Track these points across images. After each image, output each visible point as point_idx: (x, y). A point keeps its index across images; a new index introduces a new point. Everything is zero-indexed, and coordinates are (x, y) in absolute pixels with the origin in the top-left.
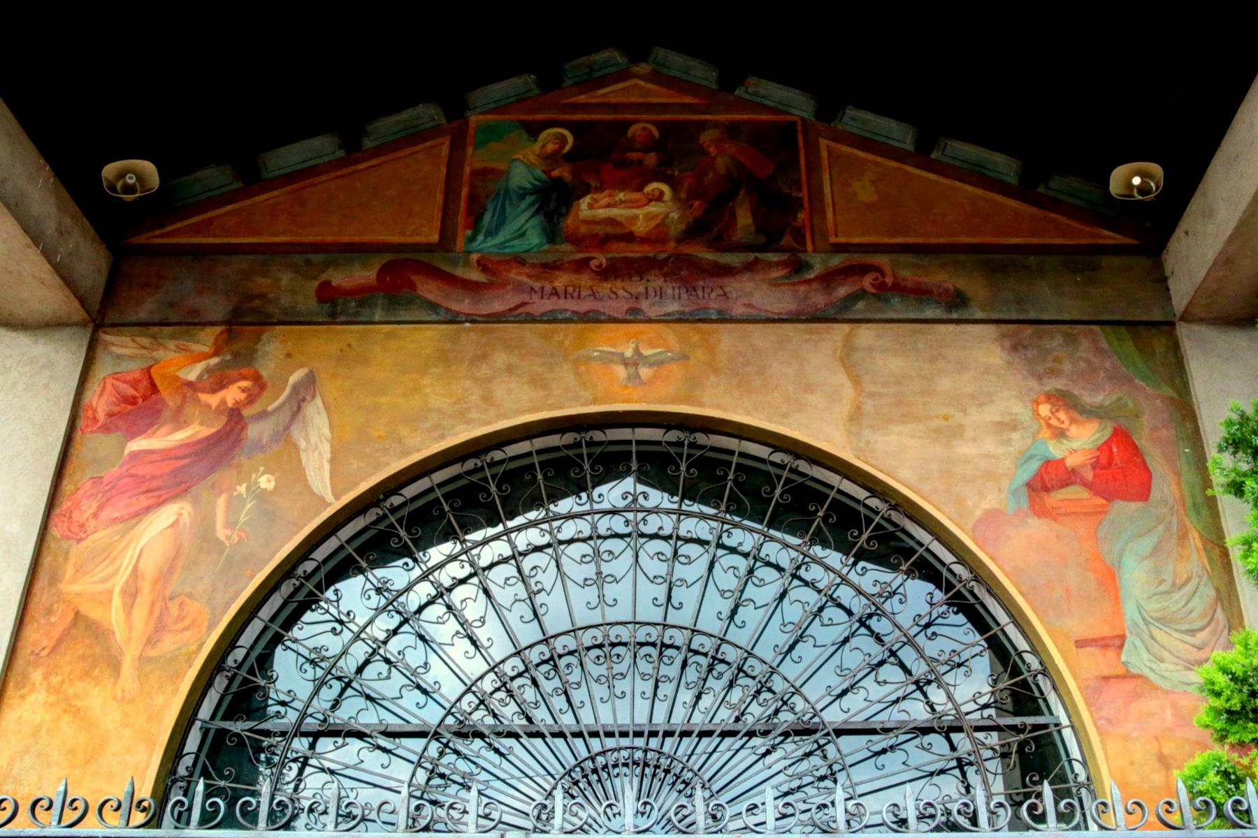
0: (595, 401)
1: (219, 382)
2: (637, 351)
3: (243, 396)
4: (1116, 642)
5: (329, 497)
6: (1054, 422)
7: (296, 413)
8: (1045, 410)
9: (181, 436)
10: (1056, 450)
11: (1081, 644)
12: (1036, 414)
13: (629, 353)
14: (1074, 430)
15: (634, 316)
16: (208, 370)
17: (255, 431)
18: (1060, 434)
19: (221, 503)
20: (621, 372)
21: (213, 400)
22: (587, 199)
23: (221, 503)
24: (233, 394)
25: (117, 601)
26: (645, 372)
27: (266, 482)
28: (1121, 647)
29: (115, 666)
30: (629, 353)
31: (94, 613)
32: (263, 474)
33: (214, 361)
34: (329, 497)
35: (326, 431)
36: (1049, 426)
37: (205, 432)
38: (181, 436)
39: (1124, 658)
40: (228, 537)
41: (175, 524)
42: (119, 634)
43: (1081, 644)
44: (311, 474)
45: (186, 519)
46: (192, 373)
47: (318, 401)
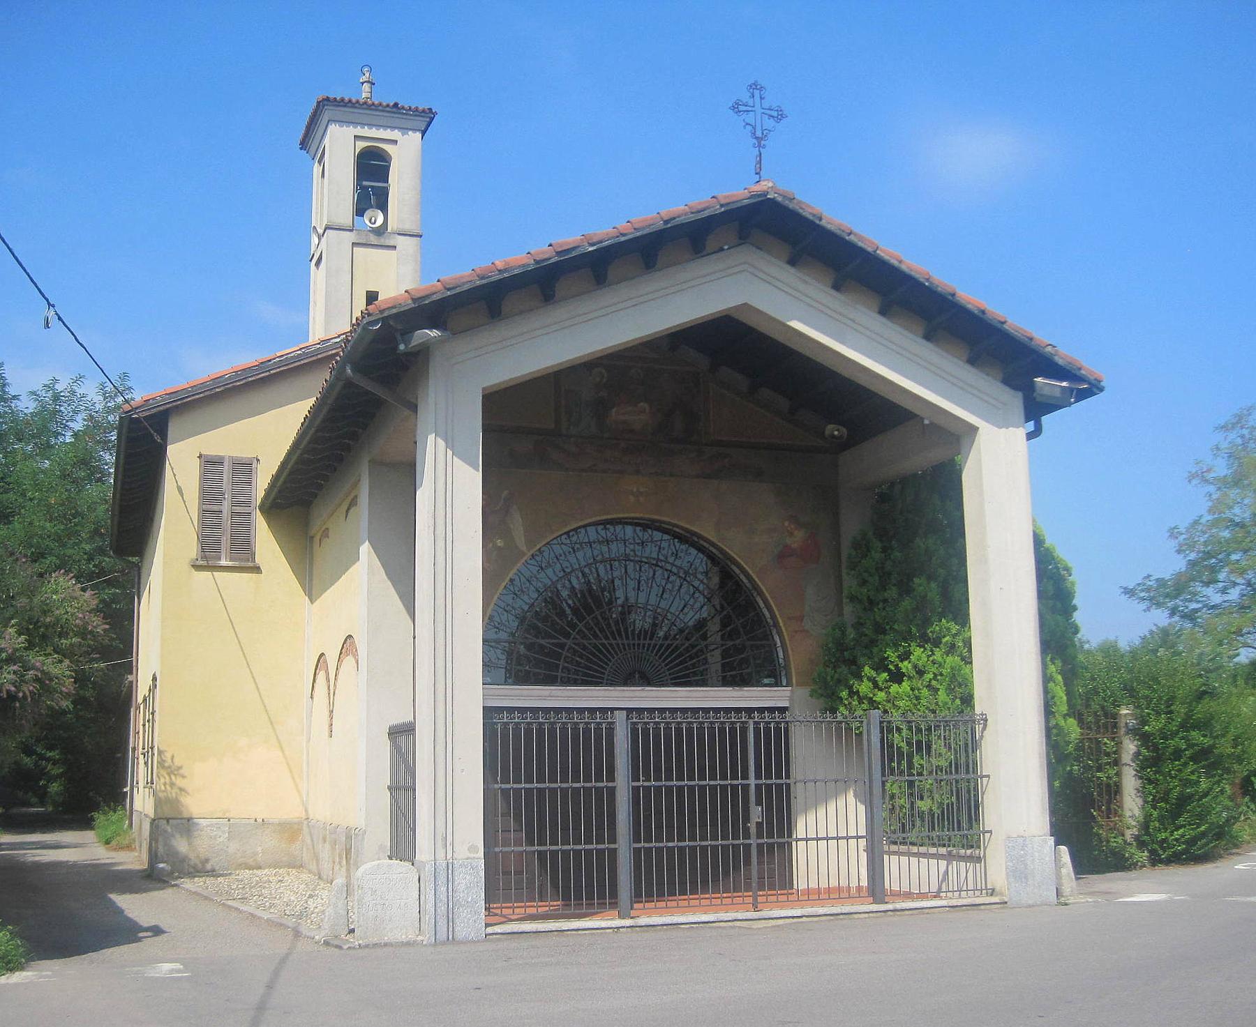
4: (801, 619)
5: (524, 549)
6: (789, 529)
8: (786, 524)
10: (788, 541)
11: (790, 619)
12: (783, 524)
13: (635, 490)
14: (796, 532)
15: (638, 472)
18: (791, 534)
20: (632, 498)
22: (614, 410)
26: (641, 499)
28: (802, 620)
30: (635, 490)
32: (498, 539)
34: (524, 549)
36: (788, 531)
39: (803, 624)
40: (489, 567)
43: (790, 619)
47: (515, 507)
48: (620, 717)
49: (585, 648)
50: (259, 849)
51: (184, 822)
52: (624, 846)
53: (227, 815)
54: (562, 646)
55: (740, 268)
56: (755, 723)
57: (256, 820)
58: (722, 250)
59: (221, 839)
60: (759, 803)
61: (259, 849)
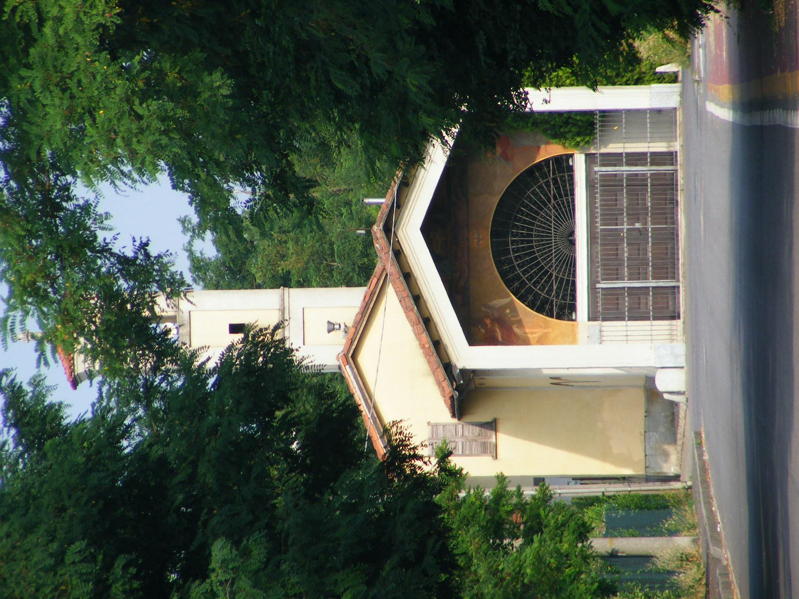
0: (488, 247)
1: (487, 325)
2: (476, 239)
3: (488, 319)
7: (492, 307)
9: (498, 330)
16: (482, 328)
17: (496, 315)
19: (512, 319)
20: (481, 242)
21: (489, 325)
23: (512, 319)
24: (488, 321)
25: (534, 336)
26: (481, 237)
27: (508, 311)
29: (546, 333)
31: (536, 339)
33: (480, 327)
35: (496, 301)
37: (497, 325)
38: (498, 330)
41: (518, 328)
42: (541, 333)
44: (506, 302)
45: (516, 325)
46: (483, 331)
47: (490, 303)
48: (598, 286)
49: (557, 266)
50: (663, 414)
51: (647, 457)
52: (652, 283)
53: (643, 433)
54: (557, 277)
55: (404, 232)
56: (601, 226)
57: (646, 416)
58: (398, 241)
59: (657, 436)
60: (634, 225)
61: (663, 414)
